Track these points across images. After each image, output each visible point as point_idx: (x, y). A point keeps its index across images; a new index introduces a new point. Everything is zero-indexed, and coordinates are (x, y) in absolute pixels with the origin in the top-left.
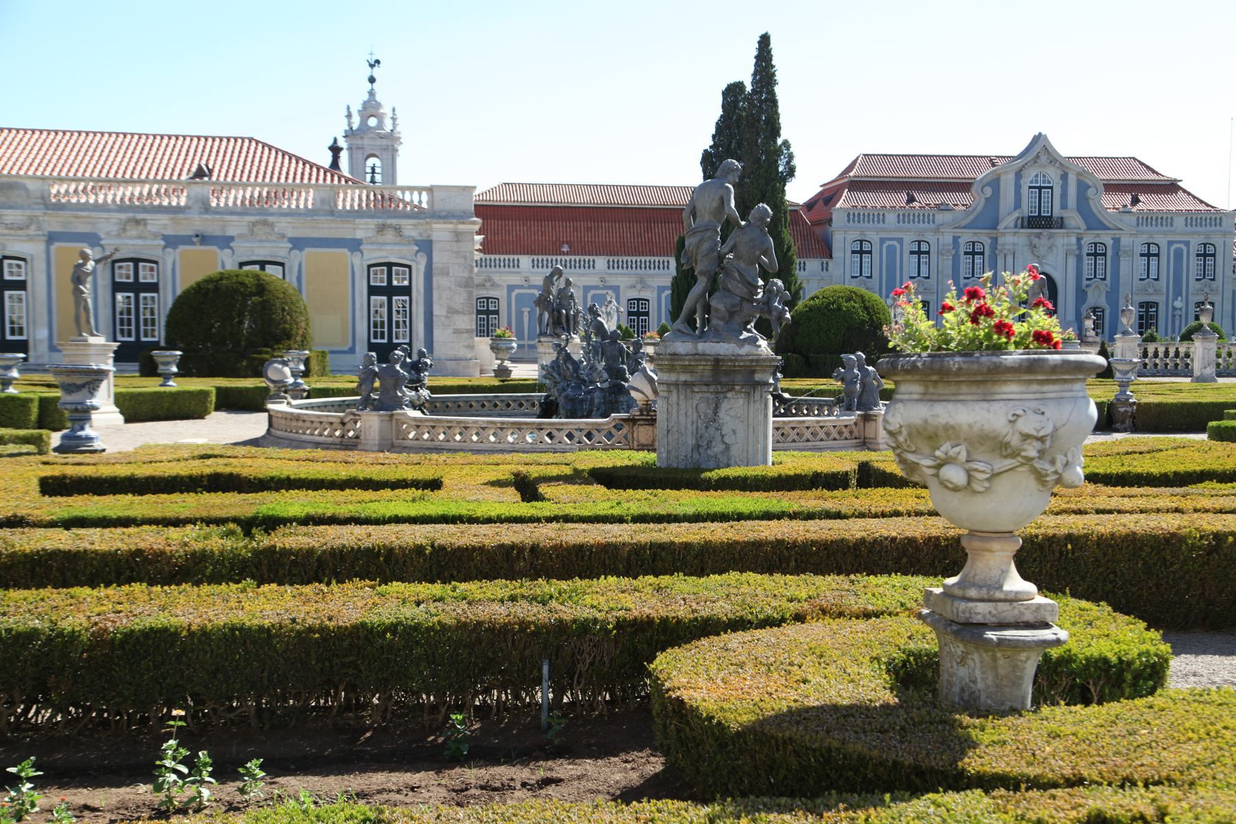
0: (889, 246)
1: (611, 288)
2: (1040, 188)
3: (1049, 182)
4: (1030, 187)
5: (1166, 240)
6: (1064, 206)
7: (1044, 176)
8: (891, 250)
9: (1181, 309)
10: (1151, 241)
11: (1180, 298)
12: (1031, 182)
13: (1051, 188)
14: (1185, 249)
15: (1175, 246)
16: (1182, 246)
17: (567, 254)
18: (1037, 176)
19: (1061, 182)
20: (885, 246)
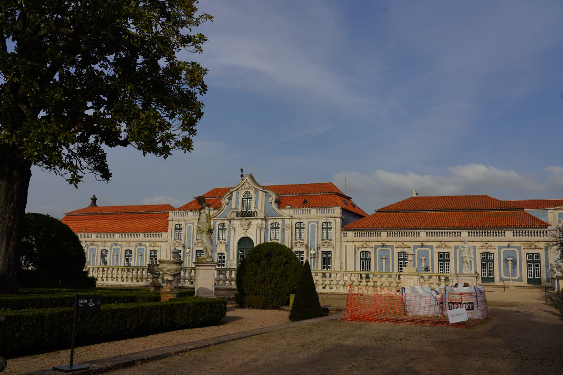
0: (190, 227)
1: (96, 245)
2: (247, 198)
3: (251, 196)
4: (243, 199)
5: (307, 220)
6: (256, 207)
7: (249, 193)
8: (190, 227)
9: (314, 255)
10: (300, 221)
11: (312, 249)
12: (244, 196)
13: (252, 198)
14: (316, 225)
15: (311, 223)
16: (315, 223)
17: (85, 232)
18: (246, 193)
19: (255, 195)
20: (187, 226)
